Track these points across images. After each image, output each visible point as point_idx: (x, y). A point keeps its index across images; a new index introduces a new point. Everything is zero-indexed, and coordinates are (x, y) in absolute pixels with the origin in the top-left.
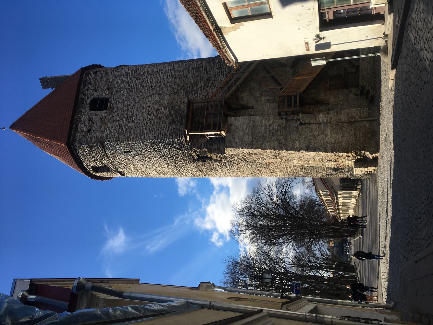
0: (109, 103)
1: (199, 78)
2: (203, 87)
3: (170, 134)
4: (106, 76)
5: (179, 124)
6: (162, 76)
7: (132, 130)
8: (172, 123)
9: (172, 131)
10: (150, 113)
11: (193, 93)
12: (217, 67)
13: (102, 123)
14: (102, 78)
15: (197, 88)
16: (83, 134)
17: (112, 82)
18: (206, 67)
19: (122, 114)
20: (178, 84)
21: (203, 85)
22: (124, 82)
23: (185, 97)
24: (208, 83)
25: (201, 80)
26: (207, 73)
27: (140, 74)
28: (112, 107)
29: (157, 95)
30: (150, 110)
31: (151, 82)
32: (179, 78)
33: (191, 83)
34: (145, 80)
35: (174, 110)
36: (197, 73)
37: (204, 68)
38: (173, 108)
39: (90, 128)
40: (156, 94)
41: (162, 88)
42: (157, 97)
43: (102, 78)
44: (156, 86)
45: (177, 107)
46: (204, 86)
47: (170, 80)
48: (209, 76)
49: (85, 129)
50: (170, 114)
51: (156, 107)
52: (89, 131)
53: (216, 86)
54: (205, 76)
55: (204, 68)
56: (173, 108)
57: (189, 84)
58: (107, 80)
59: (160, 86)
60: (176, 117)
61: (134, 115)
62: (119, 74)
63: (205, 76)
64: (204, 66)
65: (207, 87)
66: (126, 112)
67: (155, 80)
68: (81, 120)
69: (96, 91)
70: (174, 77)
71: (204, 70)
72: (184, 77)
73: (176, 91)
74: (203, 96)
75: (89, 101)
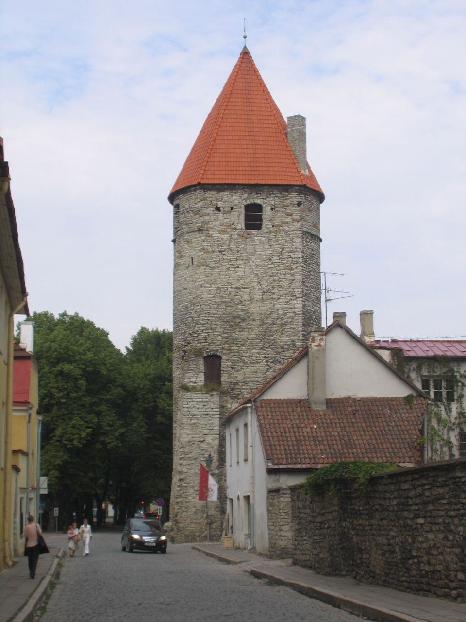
0: (254, 231)
1: (280, 350)
2: (267, 356)
3: (209, 320)
5: (222, 330)
6: (288, 300)
8: (224, 321)
9: (213, 322)
10: (238, 290)
11: (260, 344)
15: (267, 348)
16: (214, 202)
17: (283, 231)
19: (238, 252)
20: (273, 324)
21: (269, 355)
22: (283, 249)
23: (256, 335)
24: (272, 362)
25: (278, 353)
26: (286, 359)
27: (292, 269)
28: (249, 236)
29: (261, 297)
30: (242, 289)
31: (280, 286)
32: (282, 324)
35: (239, 322)
36: (286, 347)
38: (243, 320)
39: (222, 209)
44: (274, 293)
45: (243, 325)
46: (268, 357)
47: (281, 312)
48: (282, 362)
49: (220, 204)
50: (234, 317)
52: (218, 209)
54: (282, 357)
57: (272, 338)
58: (287, 223)
59: (273, 299)
60: (231, 326)
61: (237, 269)
62: (295, 240)
63: (282, 357)
65: (267, 361)
66: (241, 257)
67: (283, 291)
68: (232, 196)
69: (272, 209)
70: (284, 317)
71: (290, 355)
72: (282, 331)
73: (265, 322)
74: (256, 357)
75: (258, 201)
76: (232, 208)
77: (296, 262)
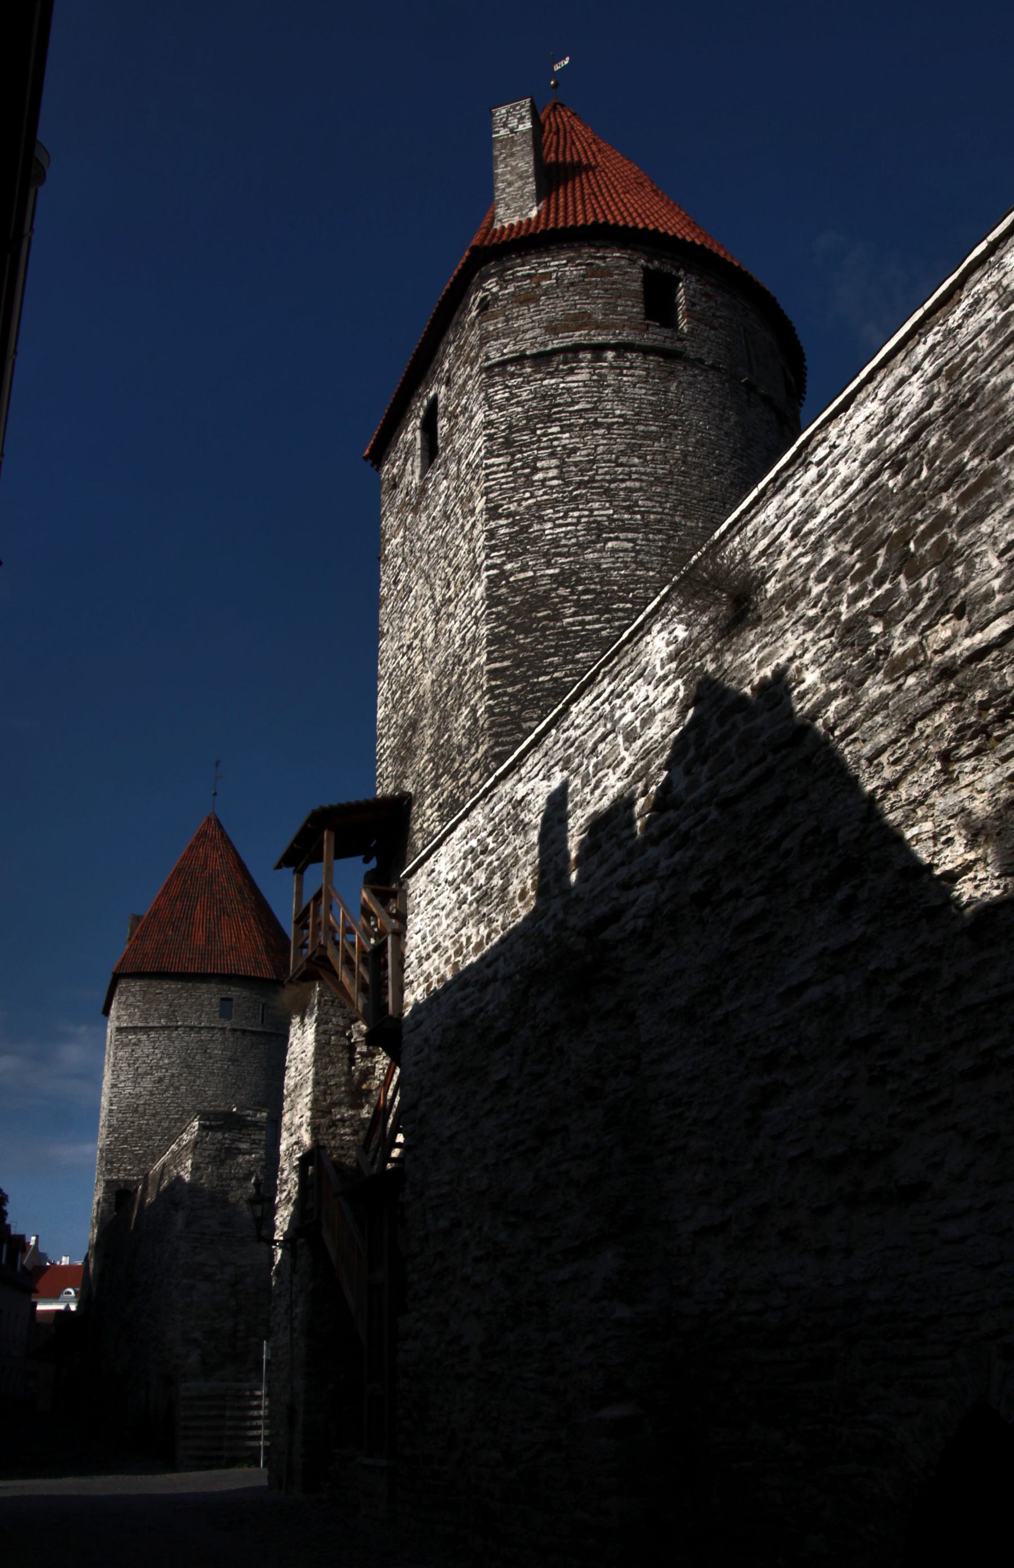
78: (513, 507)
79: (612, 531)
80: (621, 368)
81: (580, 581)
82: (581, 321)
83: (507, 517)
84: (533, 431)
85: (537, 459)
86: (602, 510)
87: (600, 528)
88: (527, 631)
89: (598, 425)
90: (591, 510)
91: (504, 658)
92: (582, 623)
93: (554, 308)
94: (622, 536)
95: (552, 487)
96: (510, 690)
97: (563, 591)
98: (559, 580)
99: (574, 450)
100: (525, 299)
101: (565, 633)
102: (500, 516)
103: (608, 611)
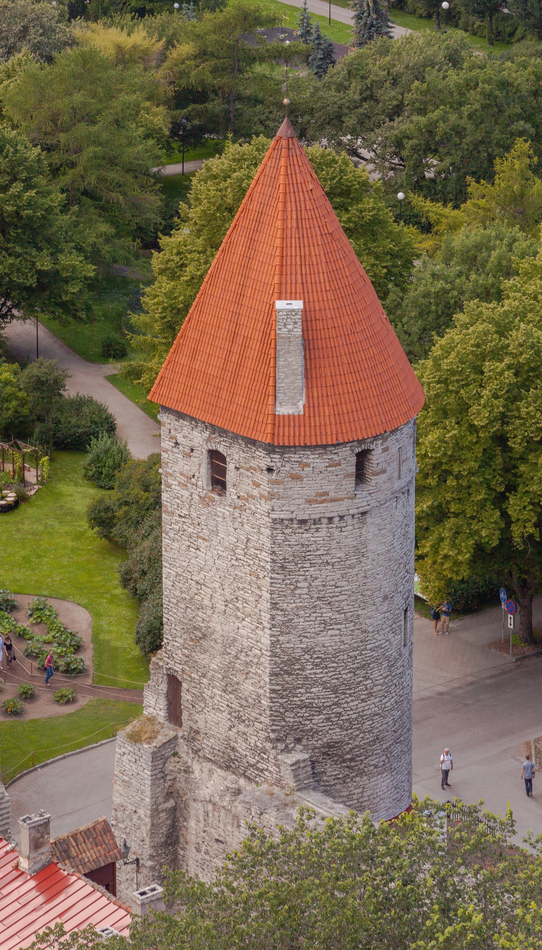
1: (244, 703)
4: (262, 496)
6: (254, 627)
7: (176, 545)
12: (258, 744)
13: (187, 477)
14: (258, 485)
18: (261, 723)
22: (248, 540)
25: (242, 706)
27: (258, 578)
33: (238, 684)
34: (249, 587)
37: (258, 716)
40: (226, 606)
41: (234, 623)
42: (220, 607)
43: (258, 485)
46: (231, 708)
48: (246, 722)
51: (206, 602)
53: (230, 730)
55: (258, 716)
56: (204, 636)
58: (253, 498)
61: (198, 552)
64: (262, 719)
65: (230, 714)
70: (249, 653)
72: (247, 673)
73: (228, 650)
75: (221, 449)
76: (192, 450)
77: (264, 567)
78: (285, 606)
79: (331, 625)
80: (341, 527)
81: (314, 652)
82: (323, 497)
83: (282, 610)
84: (296, 564)
85: (297, 581)
86: (328, 615)
87: (325, 622)
88: (289, 674)
89: (328, 563)
90: (322, 613)
91: (278, 685)
92: (315, 673)
93: (308, 488)
94: (336, 627)
95: (304, 599)
96: (280, 701)
97: (307, 657)
98: (306, 651)
99: (316, 578)
100: (296, 478)
101: (306, 678)
102: (278, 609)
103: (326, 667)
